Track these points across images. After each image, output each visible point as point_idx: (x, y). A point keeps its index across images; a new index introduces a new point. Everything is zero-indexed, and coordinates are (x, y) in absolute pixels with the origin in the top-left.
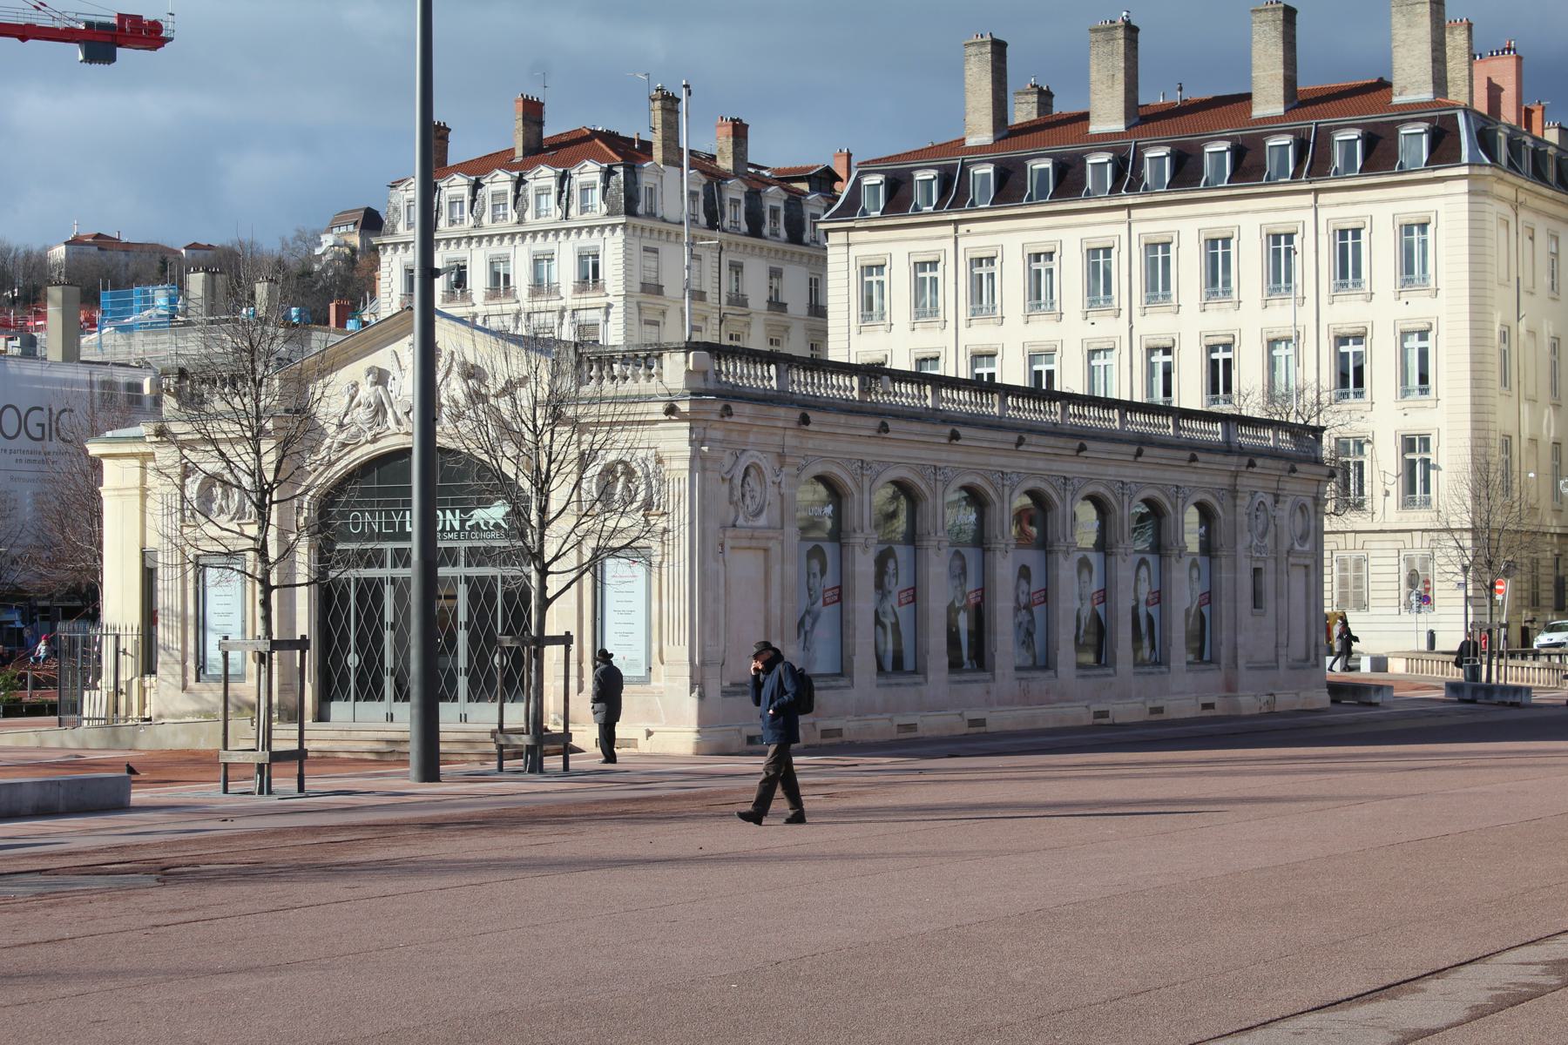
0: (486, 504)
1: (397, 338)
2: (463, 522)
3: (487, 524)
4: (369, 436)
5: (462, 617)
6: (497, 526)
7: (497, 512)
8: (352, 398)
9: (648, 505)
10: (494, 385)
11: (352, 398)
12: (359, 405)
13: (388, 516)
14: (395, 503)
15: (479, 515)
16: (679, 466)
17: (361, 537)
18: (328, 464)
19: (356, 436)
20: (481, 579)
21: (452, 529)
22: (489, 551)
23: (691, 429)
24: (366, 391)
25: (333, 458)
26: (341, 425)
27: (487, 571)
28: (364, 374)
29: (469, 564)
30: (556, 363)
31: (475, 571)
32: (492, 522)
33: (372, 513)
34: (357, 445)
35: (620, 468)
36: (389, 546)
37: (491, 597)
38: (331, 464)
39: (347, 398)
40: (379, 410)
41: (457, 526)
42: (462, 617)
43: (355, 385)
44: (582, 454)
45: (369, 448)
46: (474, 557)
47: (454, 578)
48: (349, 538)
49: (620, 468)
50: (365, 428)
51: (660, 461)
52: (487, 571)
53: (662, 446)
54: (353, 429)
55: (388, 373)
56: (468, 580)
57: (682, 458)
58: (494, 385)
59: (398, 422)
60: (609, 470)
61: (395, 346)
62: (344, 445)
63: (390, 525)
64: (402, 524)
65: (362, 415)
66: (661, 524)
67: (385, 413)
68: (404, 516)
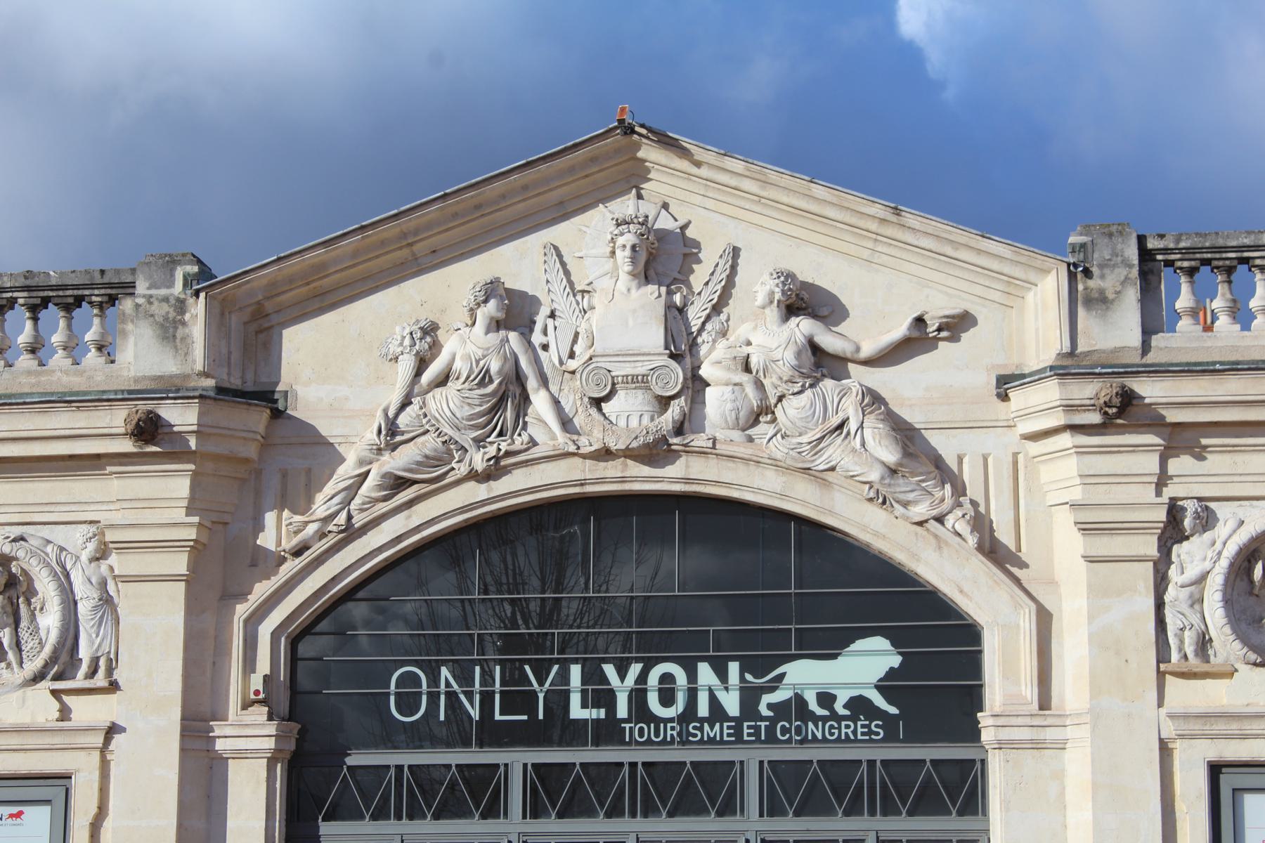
0: (828, 645)
1: (562, 212)
2: (750, 697)
3: (826, 699)
4: (479, 460)
6: (859, 706)
7: (865, 665)
8: (422, 364)
10: (869, 329)
11: (422, 364)
12: (443, 380)
13: (514, 675)
14: (539, 643)
15: (804, 675)
16: (575, 699)
17: (419, 736)
18: (315, 547)
19: (433, 461)
21: (717, 710)
22: (839, 772)
24: (469, 346)
25: (358, 521)
26: (391, 434)
28: (467, 297)
29: (772, 808)
30: (1078, 271)
32: (842, 697)
33: (464, 677)
34: (438, 485)
36: (517, 760)
38: (351, 533)
39: (407, 365)
40: (508, 395)
41: (731, 703)
43: (430, 330)
44: (1174, 511)
45: (480, 491)
48: (390, 736)
50: (466, 438)
54: (429, 443)
55: (534, 302)
58: (869, 329)
59: (566, 424)
61: (560, 233)
62: (397, 483)
63: (519, 700)
64: (559, 699)
65: (450, 405)
67: (525, 400)
68: (564, 677)
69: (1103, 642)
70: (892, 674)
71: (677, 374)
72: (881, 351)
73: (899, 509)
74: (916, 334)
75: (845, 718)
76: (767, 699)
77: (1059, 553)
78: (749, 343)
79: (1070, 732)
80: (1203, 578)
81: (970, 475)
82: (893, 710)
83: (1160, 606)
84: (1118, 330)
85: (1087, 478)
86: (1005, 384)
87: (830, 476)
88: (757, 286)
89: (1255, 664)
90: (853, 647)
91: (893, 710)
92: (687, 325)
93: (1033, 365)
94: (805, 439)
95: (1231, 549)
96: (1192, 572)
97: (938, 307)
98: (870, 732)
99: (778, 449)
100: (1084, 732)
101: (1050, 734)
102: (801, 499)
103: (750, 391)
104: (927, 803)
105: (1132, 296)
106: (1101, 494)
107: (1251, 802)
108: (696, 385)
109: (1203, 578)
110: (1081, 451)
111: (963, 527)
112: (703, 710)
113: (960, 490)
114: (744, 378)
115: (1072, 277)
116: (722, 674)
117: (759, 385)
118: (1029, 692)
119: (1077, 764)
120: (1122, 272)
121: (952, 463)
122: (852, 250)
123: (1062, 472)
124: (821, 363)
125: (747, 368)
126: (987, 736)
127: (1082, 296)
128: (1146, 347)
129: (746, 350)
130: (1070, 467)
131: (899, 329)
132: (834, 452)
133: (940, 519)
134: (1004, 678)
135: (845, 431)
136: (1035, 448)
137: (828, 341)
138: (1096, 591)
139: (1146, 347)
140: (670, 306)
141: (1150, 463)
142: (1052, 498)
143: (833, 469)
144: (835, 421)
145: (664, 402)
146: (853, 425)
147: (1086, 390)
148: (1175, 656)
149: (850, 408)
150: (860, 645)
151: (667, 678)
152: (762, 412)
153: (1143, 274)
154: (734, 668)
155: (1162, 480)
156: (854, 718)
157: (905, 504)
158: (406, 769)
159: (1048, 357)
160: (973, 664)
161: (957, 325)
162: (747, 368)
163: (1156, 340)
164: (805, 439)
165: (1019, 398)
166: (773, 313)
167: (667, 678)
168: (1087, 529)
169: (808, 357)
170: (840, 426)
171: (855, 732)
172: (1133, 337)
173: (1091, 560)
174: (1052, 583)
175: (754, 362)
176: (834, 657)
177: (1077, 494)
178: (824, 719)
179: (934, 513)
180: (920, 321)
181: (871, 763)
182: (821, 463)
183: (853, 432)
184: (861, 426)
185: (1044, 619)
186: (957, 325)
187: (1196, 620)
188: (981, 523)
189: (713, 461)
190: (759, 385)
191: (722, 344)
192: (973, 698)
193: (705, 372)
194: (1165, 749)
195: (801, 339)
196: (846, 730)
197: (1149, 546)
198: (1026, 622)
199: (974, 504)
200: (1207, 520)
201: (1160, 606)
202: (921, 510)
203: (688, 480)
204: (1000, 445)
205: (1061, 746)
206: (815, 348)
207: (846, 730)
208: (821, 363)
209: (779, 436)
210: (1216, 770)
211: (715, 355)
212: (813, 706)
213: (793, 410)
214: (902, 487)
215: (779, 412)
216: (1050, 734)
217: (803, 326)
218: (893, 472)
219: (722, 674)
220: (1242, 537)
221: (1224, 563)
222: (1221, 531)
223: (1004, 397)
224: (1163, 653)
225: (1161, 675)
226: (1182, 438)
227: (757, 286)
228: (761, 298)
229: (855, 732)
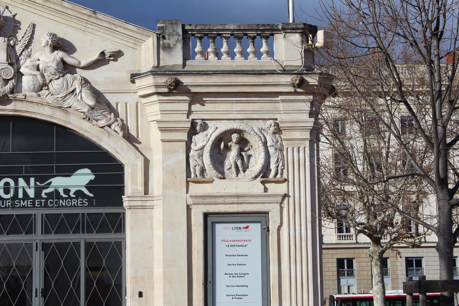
0: (68, 172)
2: (38, 191)
3: (67, 191)
5: (38, 283)
6: (79, 194)
7: (81, 179)
9: (265, 171)
15: (59, 182)
20: (62, 246)
22: (71, 218)
23: (312, 103)
27: (69, 238)
29: (46, 231)
30: (160, 37)
31: (53, 238)
32: (73, 190)
35: (235, 137)
37: (73, 265)
41: (31, 193)
42: (38, 283)
44: (193, 124)
46: (54, 224)
47: (29, 246)
49: (235, 137)
51: (278, 130)
52: (69, 238)
53: (280, 117)
56: (45, 247)
57: (303, 129)
60: (224, 137)
66: (281, 189)
69: (168, 171)
70: (91, 182)
71: (11, 71)
72: (88, 64)
73: (94, 122)
74: (101, 58)
75: (74, 198)
76: (45, 191)
77: (152, 138)
78: (39, 60)
79: (155, 203)
80: (203, 148)
81: (121, 110)
82: (91, 195)
83: (188, 157)
84: (175, 58)
85: (163, 112)
86: (134, 77)
87: (69, 110)
88: (42, 39)
89: (221, 178)
90: (77, 172)
91: (91, 195)
92: (15, 53)
93: (144, 70)
94: (60, 96)
95: (213, 137)
96: (199, 146)
97: (110, 48)
98: (83, 203)
99: (50, 99)
100: (160, 202)
101: (148, 203)
102: (58, 118)
103: (39, 78)
104: (103, 229)
105: (179, 46)
106: (168, 117)
107: (219, 227)
108: (18, 75)
109: (203, 148)
110: (161, 102)
111: (118, 129)
112: (21, 195)
113: (117, 115)
114: (37, 73)
115: (158, 39)
116: (28, 183)
117: (43, 76)
118: (141, 188)
119: (157, 214)
120: (176, 38)
121: (114, 105)
122: (78, 26)
123: (153, 109)
124: (66, 68)
125: (38, 69)
126: (125, 204)
127: (162, 46)
128: (184, 65)
129: (38, 62)
130: (157, 107)
131: (95, 56)
132: (71, 101)
133: (109, 126)
134: (132, 183)
135: (75, 93)
136: (144, 100)
137: (69, 60)
138: (165, 152)
139: (184, 65)
140: (9, 45)
141: (185, 106)
142: (150, 119)
143: (70, 107)
144: (71, 89)
145: (6, 81)
146: (78, 91)
147: (163, 80)
148: (193, 176)
149: (77, 85)
150: (79, 171)
151: (7, 184)
152: (44, 85)
153: (184, 38)
154: (32, 180)
155: (189, 112)
156: (77, 198)
157: (97, 120)
158: (86, 214)
159: (149, 67)
160: (121, 179)
161: (117, 55)
162: (38, 69)
163: (188, 62)
164: (60, 96)
165: (139, 82)
166: (48, 49)
167: (7, 184)
168: (162, 130)
169: (61, 65)
170: (73, 91)
171: (77, 203)
172: (180, 61)
173: (164, 141)
174: (150, 149)
175: (41, 67)
176: (70, 176)
177: (159, 117)
178: (66, 199)
179: (107, 123)
180: (103, 53)
181: (83, 214)
182: (66, 105)
183: (78, 94)
184: (81, 92)
185: (147, 162)
186: (117, 55)
187: (200, 162)
188: (124, 127)
189: (25, 104)
190: (43, 76)
191: (29, 60)
192: (121, 191)
193: (22, 70)
194: (189, 209)
195: (58, 59)
196: (74, 202)
197: (184, 136)
198: (140, 163)
199: (122, 120)
200: (205, 127)
201: (188, 157)
202: (103, 122)
203: (15, 111)
204: (131, 99)
205: (152, 208)
206: (63, 62)
207: (74, 202)
208: (66, 68)
209: (50, 95)
210: (206, 215)
211: (26, 64)
212: (62, 194)
213: (55, 85)
214: (95, 114)
215: (50, 86)
216: (148, 203)
217: (59, 54)
218: (92, 108)
219: (28, 183)
220: (217, 133)
221: (210, 142)
222: (210, 131)
223: (133, 82)
224: (188, 174)
225: (188, 182)
226: (197, 98)
227: (42, 39)
228: (43, 43)
229: (77, 203)
